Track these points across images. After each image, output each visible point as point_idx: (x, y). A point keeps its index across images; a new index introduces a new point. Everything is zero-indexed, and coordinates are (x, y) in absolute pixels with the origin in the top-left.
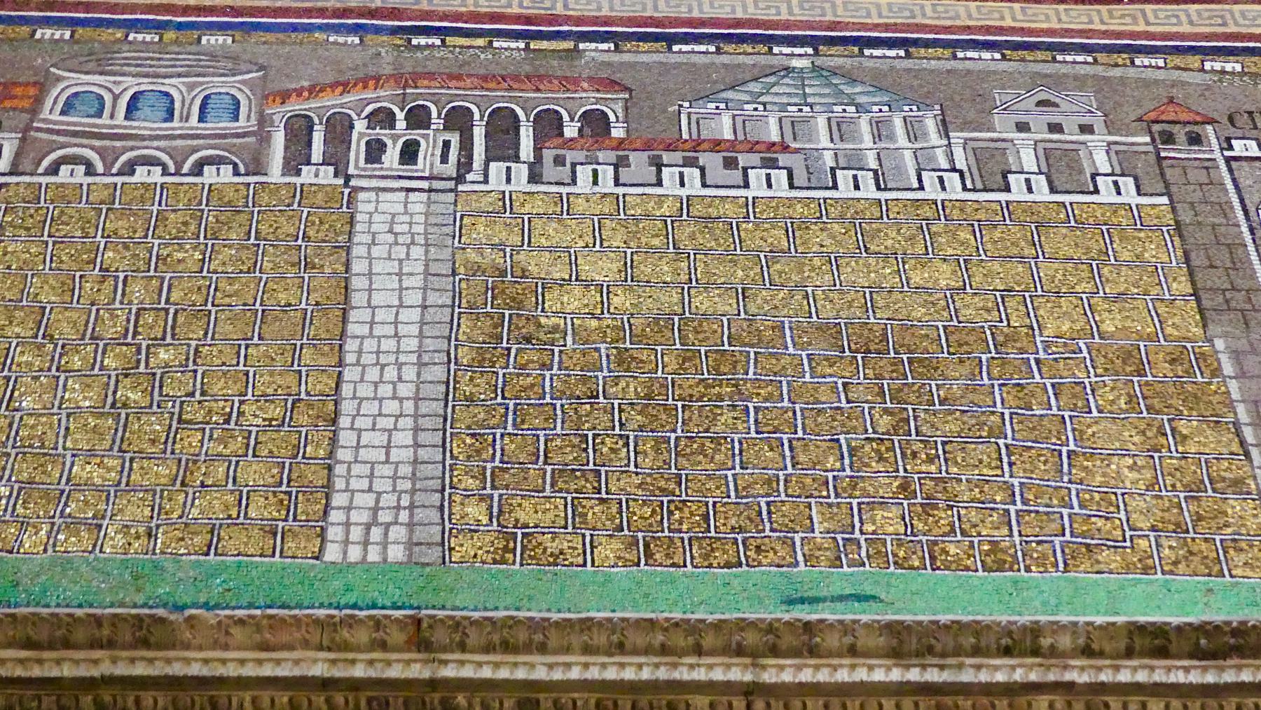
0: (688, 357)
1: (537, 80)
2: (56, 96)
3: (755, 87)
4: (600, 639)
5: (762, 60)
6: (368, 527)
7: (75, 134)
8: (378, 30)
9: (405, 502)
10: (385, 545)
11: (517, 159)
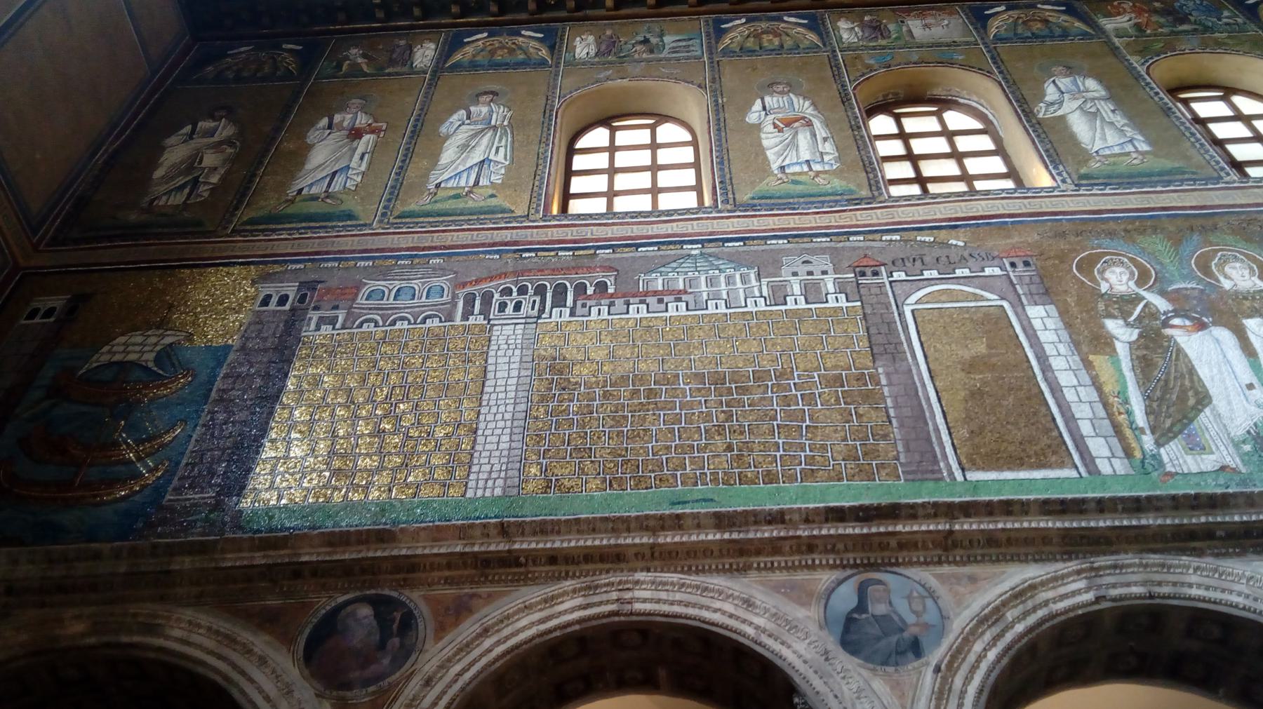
1: (576, 269)
6: (487, 480)
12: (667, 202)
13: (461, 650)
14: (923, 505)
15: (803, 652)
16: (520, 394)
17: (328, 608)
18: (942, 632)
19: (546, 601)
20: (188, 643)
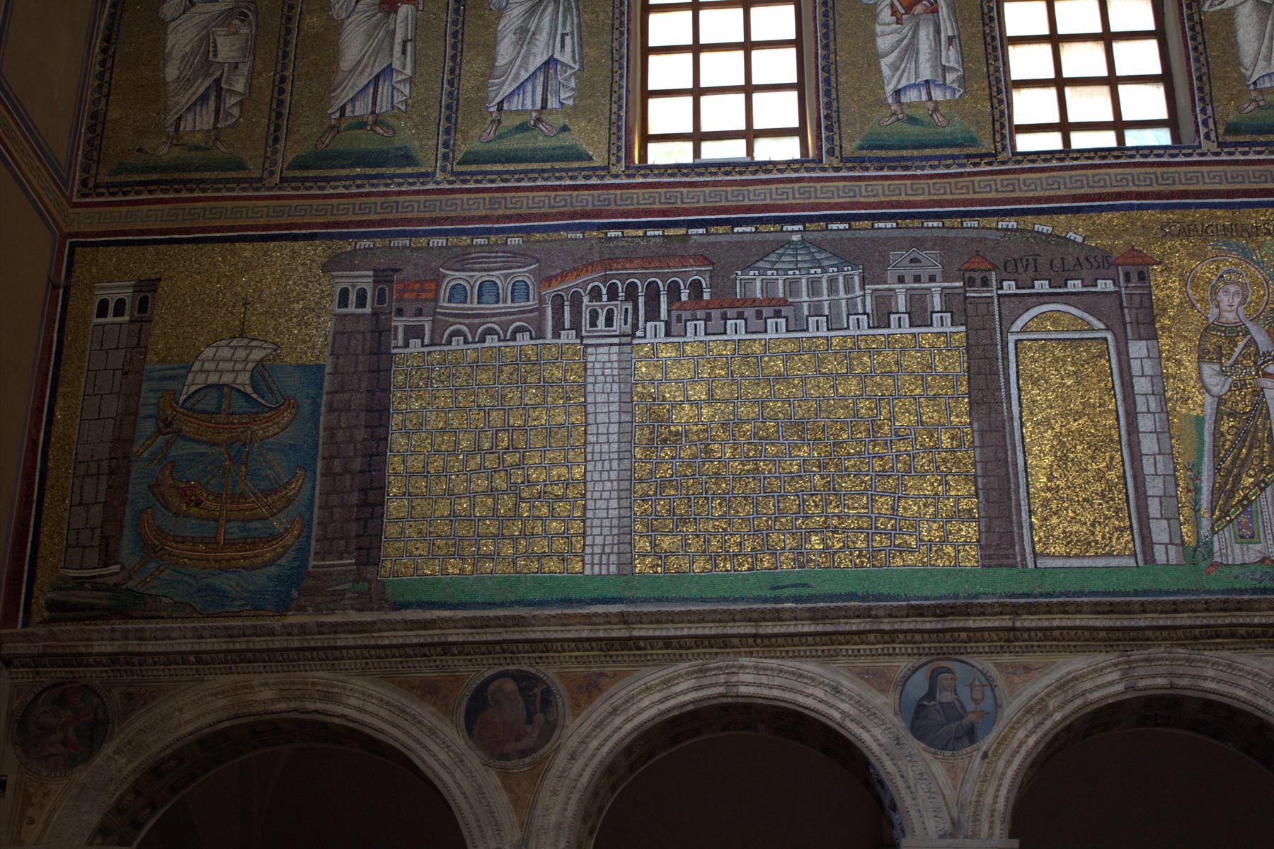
3: (773, 257)
4: (695, 618)
5: (779, 236)
6: (601, 554)
7: (457, 316)
10: (608, 565)
11: (657, 318)
12: (766, 150)
13: (596, 727)
14: (992, 605)
15: (879, 737)
16: (624, 447)
18: (991, 719)
19: (664, 683)
20: (366, 712)
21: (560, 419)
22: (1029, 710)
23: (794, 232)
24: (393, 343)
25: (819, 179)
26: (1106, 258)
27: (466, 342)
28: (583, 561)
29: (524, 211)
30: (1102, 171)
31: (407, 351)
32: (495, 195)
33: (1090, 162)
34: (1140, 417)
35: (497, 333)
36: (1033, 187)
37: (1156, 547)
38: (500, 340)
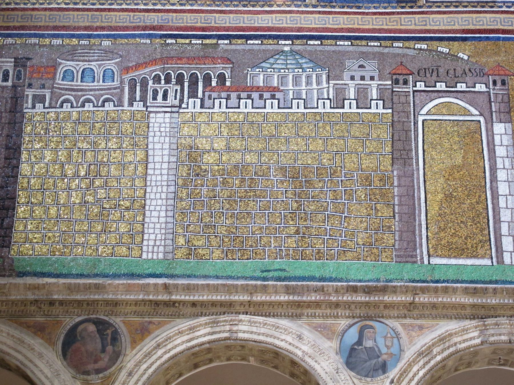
0: (243, 180)
2: (60, 71)
3: (272, 61)
5: (276, 47)
6: (153, 246)
7: (66, 89)
8: (156, 36)
9: (163, 238)
10: (158, 253)
13: (146, 356)
15: (326, 368)
16: (172, 178)
17: (71, 325)
19: (190, 329)
21: (130, 158)
22: (421, 354)
23: (286, 45)
24: (25, 105)
25: (303, 12)
26: (481, 70)
27: (72, 107)
28: (141, 249)
29: (113, 24)
30: (482, 15)
31: (34, 110)
32: (96, 13)
33: (474, 9)
34: (498, 171)
35: (93, 102)
36: (438, 23)
37: (505, 253)
38: (94, 106)
